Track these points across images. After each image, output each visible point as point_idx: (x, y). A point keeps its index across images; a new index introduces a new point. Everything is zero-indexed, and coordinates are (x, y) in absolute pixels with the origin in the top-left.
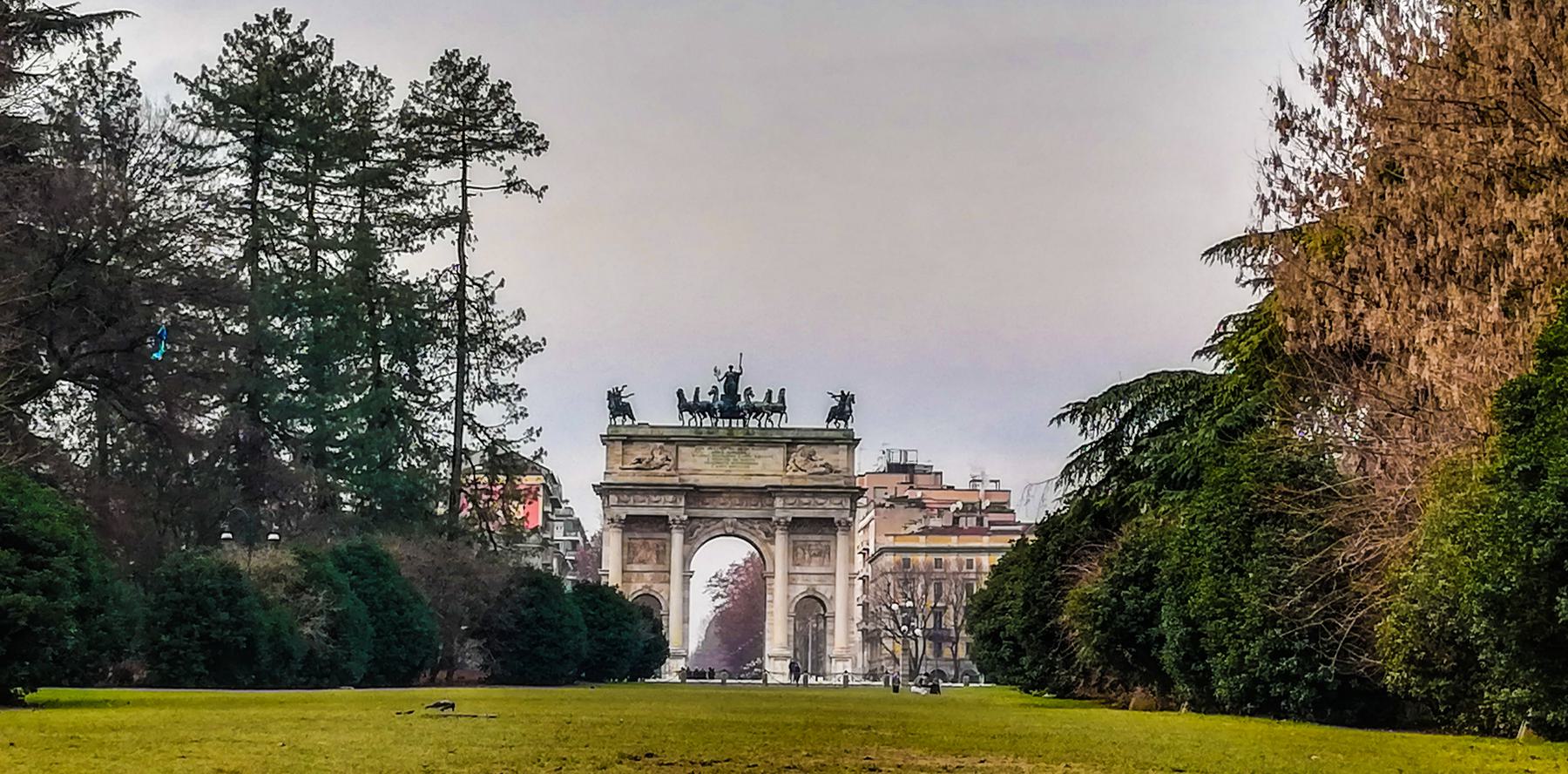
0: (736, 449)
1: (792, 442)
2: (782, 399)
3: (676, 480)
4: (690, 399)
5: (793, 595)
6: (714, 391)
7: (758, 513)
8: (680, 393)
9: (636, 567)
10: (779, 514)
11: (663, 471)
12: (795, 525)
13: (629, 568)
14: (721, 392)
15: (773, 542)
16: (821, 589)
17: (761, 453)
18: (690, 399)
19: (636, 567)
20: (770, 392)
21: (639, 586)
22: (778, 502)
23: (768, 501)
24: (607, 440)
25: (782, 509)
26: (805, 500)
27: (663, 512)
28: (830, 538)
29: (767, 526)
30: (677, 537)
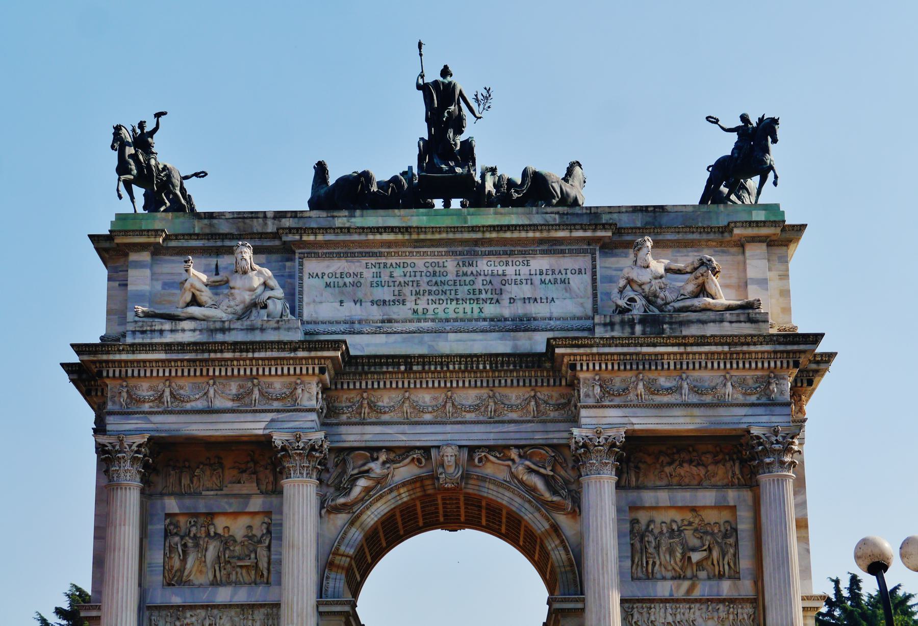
12: (638, 456)
24: (111, 248)
28: (732, 496)
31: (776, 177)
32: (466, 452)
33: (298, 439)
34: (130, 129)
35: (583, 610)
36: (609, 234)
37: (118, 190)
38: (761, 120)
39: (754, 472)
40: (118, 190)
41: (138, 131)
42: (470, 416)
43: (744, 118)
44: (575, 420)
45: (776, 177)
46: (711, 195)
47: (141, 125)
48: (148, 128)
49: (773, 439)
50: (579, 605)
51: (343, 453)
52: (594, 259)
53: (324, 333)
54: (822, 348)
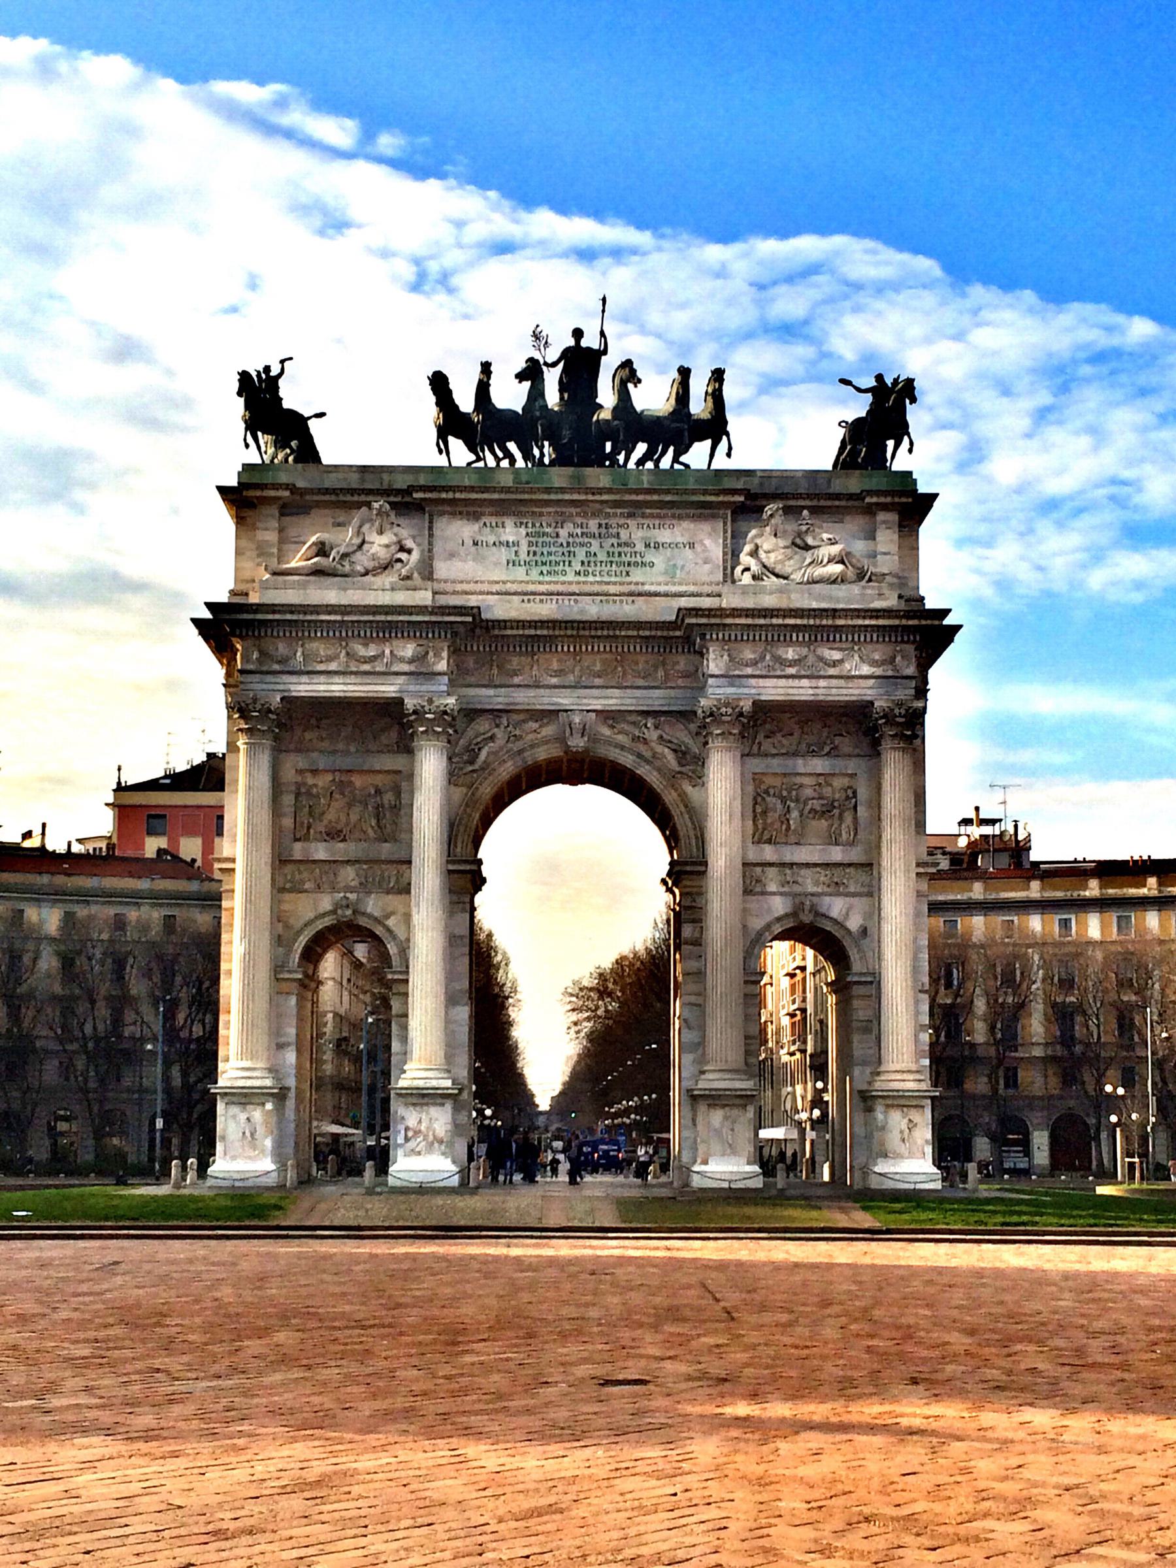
0: (593, 525)
1: (746, 500)
2: (717, 398)
3: (424, 597)
4: (465, 401)
5: (757, 924)
6: (532, 372)
7: (656, 699)
8: (439, 383)
9: (321, 852)
10: (716, 692)
11: (388, 579)
13: (298, 850)
14: (552, 397)
15: (698, 778)
16: (836, 907)
17: (664, 535)
18: (465, 401)
19: (321, 852)
20: (685, 373)
21: (326, 903)
22: (715, 663)
23: (682, 662)
25: (730, 679)
26: (790, 653)
27: (388, 689)
28: (852, 766)
29: (681, 734)
30: (431, 765)
31: (911, 443)
32: (594, 714)
33: (430, 701)
34: (254, 374)
35: (704, 872)
36: (742, 499)
37: (245, 440)
38: (896, 381)
39: (875, 744)
40: (245, 440)
41: (264, 376)
42: (598, 682)
43: (879, 378)
44: (702, 688)
45: (911, 443)
46: (846, 461)
47: (267, 369)
48: (273, 373)
49: (897, 711)
50: (703, 869)
51: (471, 714)
52: (725, 524)
53: (455, 593)
54: (948, 621)
